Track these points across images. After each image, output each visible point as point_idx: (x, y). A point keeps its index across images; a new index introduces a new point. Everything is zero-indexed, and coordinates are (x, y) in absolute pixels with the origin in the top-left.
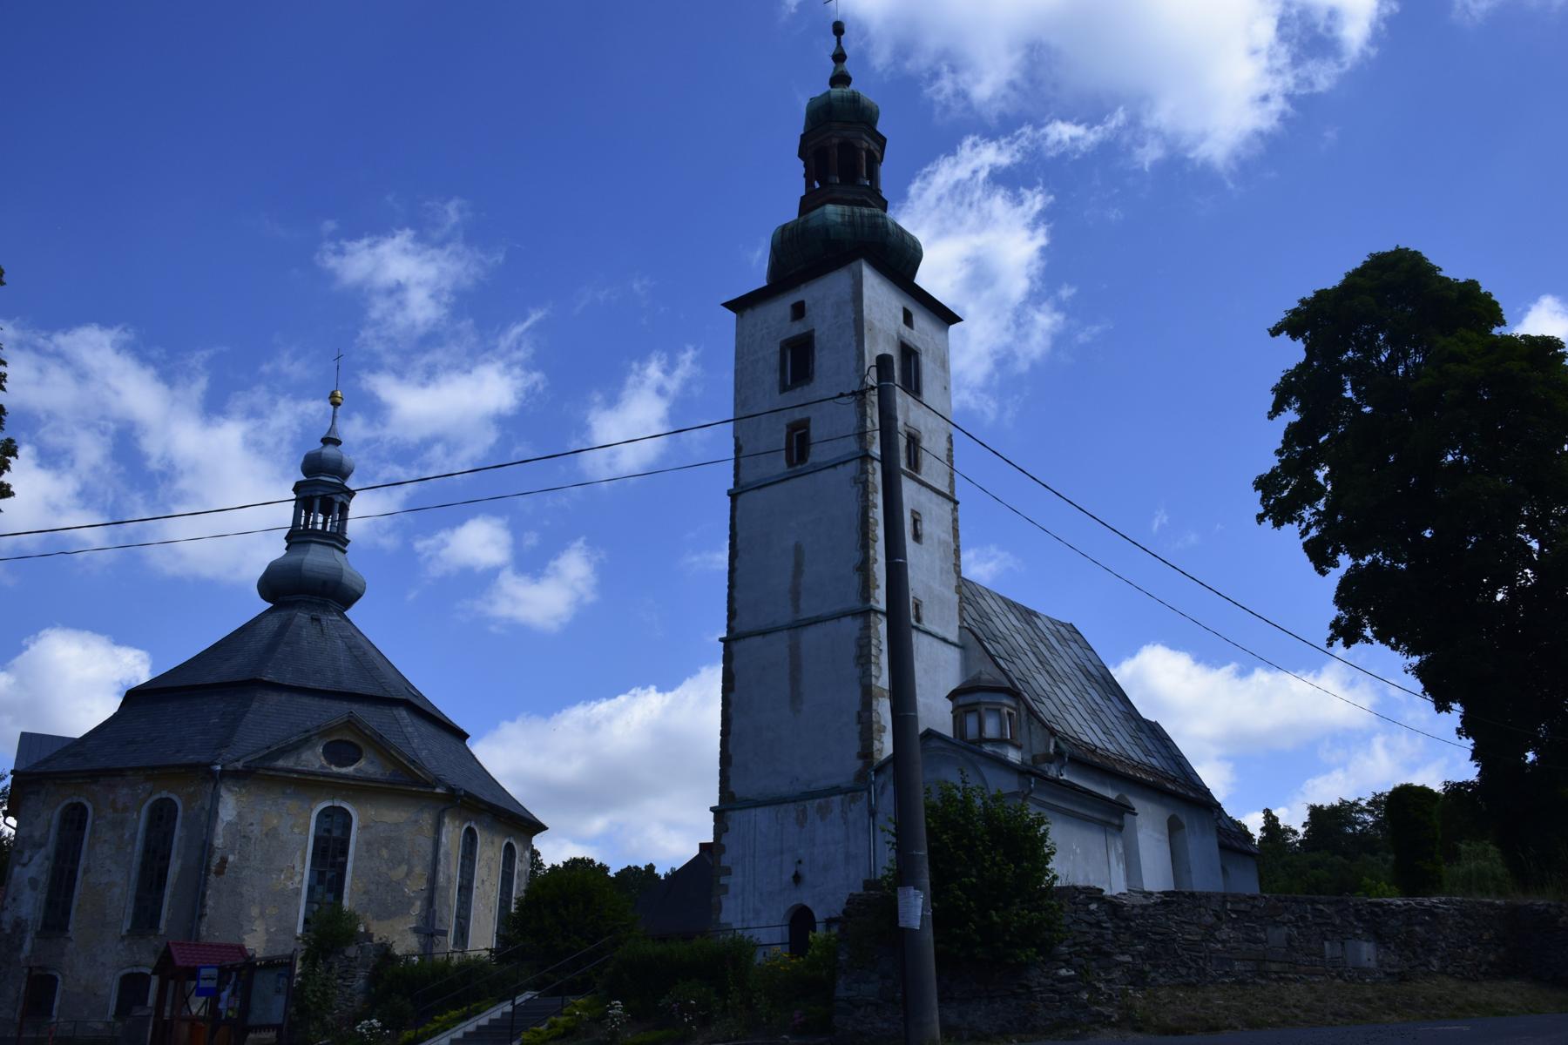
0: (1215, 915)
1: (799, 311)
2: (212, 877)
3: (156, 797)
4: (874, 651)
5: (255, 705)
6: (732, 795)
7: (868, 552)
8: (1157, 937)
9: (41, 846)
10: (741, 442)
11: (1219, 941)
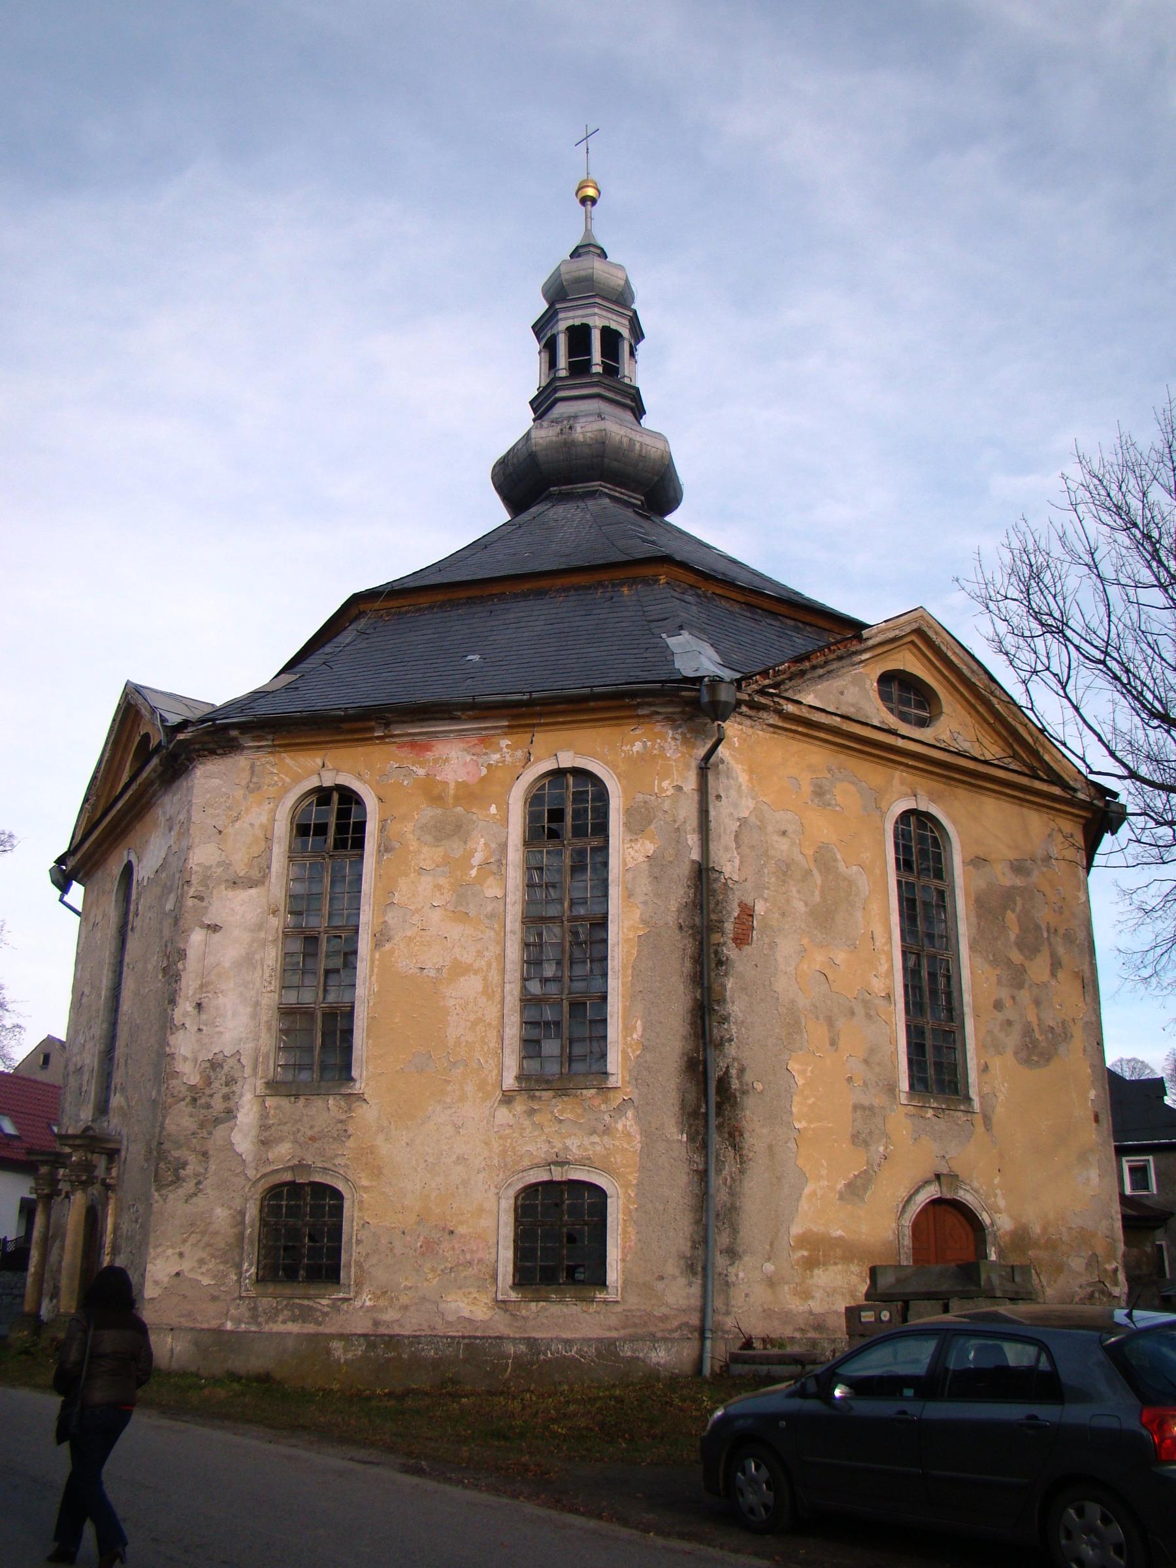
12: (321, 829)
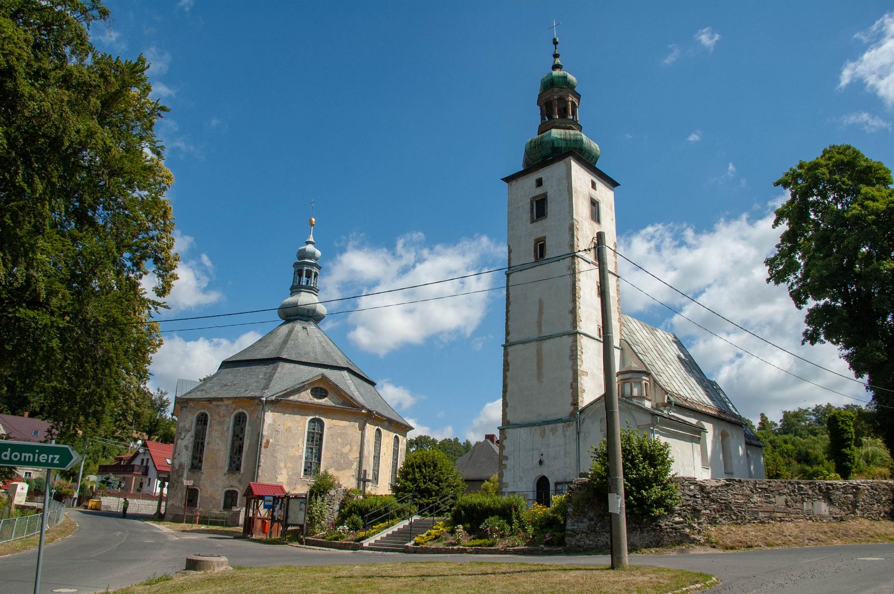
0: (751, 490)
1: (539, 183)
2: (263, 449)
3: (237, 411)
4: (579, 353)
5: (279, 369)
6: (508, 422)
7: (576, 303)
8: (723, 501)
9: (189, 431)
10: (511, 248)
11: (752, 503)
12: (202, 421)
